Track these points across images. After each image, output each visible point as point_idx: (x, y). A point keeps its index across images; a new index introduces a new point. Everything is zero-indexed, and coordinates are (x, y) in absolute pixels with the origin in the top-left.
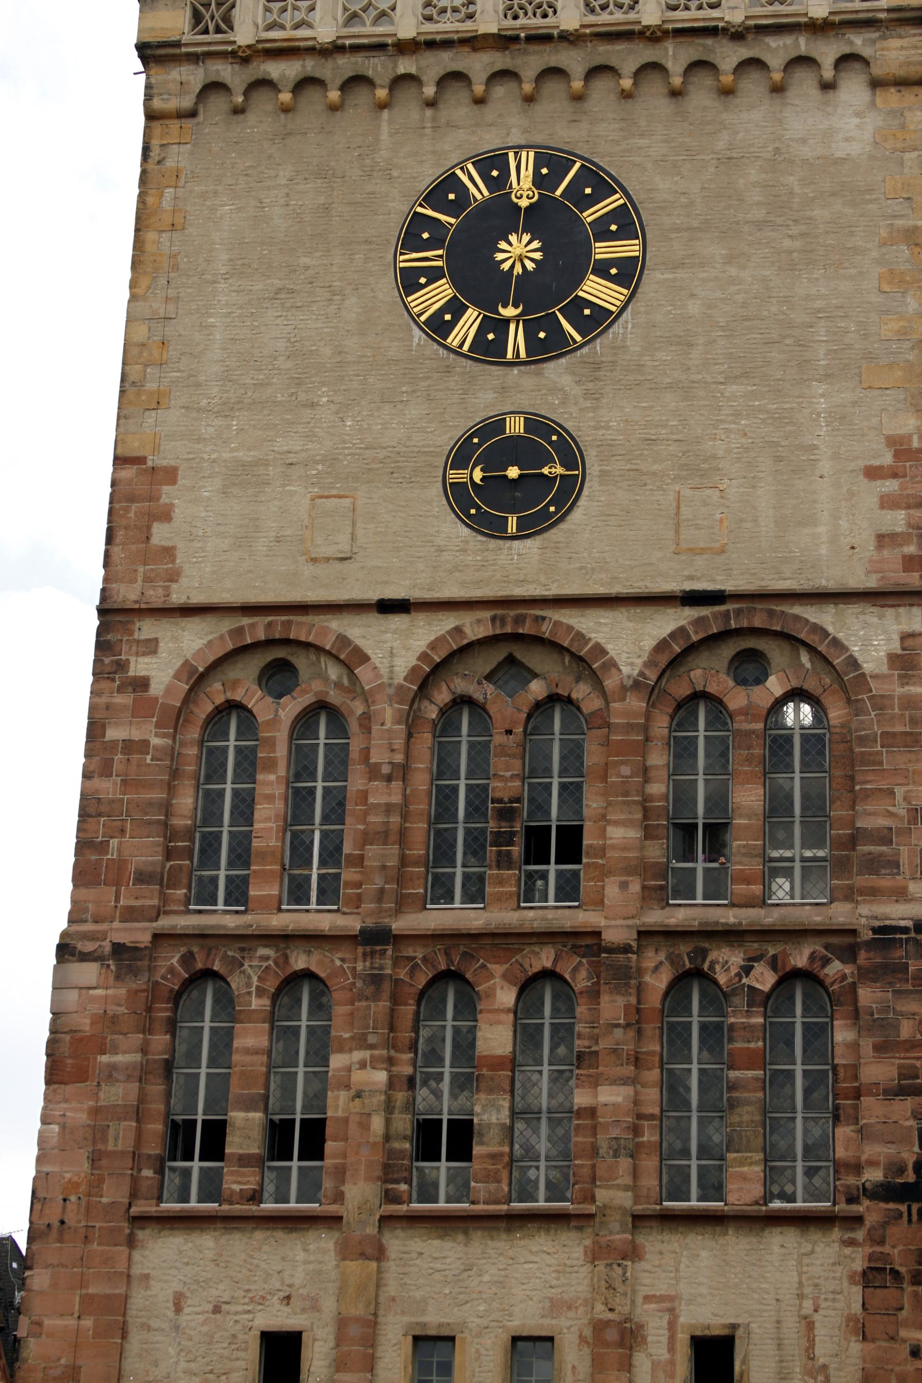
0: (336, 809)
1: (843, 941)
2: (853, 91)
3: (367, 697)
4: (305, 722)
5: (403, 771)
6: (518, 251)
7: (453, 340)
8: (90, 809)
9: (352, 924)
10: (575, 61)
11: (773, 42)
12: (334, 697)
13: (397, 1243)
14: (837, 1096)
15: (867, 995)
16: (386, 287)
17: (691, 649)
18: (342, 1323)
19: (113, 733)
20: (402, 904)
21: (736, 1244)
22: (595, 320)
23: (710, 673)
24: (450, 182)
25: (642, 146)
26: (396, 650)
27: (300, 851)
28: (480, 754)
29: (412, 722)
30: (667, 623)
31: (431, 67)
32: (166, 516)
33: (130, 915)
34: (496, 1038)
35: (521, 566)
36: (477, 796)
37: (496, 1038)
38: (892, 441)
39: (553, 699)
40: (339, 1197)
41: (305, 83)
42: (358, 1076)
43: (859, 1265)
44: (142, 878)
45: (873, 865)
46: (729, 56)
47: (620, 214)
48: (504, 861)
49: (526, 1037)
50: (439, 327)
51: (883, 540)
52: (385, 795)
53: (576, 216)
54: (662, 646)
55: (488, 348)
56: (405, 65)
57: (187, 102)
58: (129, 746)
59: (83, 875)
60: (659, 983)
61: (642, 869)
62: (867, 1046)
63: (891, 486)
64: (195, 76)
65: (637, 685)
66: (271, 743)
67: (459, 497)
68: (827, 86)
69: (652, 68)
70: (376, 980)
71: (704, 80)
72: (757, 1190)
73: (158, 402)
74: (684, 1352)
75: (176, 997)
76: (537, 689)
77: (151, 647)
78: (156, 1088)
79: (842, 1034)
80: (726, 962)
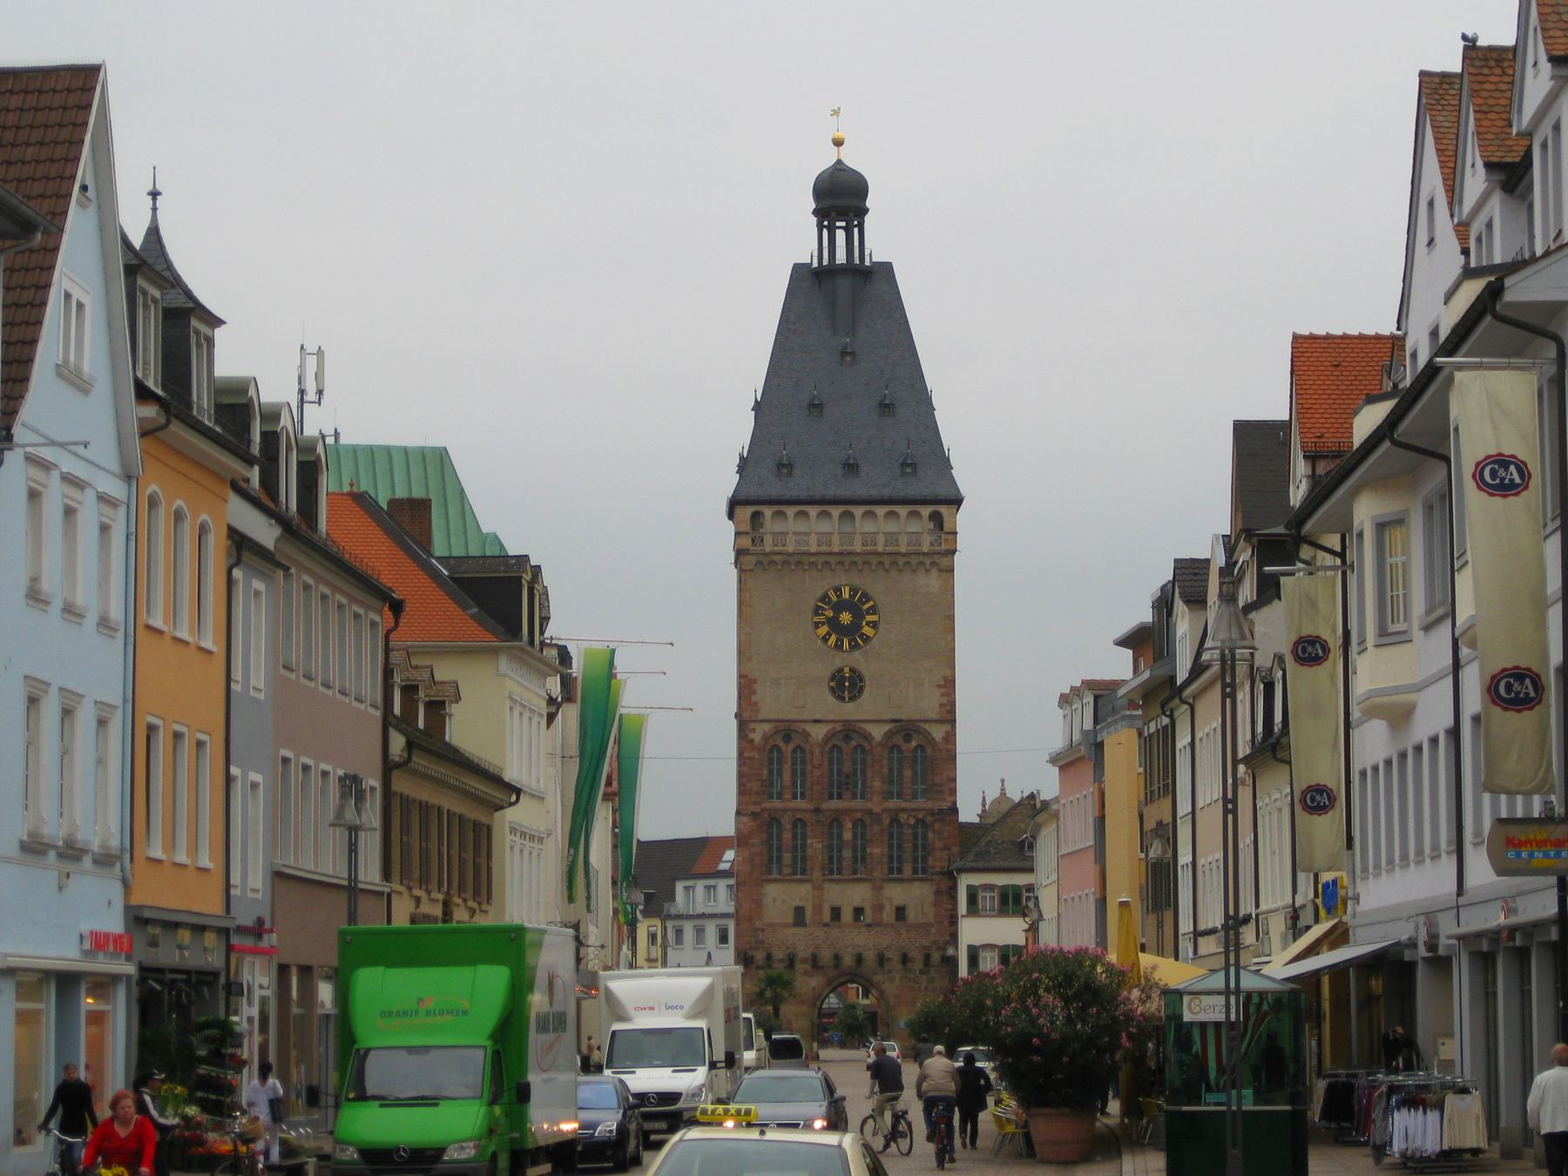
0: (803, 774)
1: (932, 813)
2: (934, 573)
4: (794, 751)
6: (846, 618)
8: (740, 775)
9: (810, 806)
10: (859, 559)
13: (826, 885)
15: (937, 826)
16: (810, 626)
21: (906, 886)
22: (867, 639)
23: (898, 740)
24: (826, 595)
26: (818, 732)
27: (794, 784)
28: (839, 760)
29: (822, 753)
33: (755, 803)
34: (848, 835)
35: (850, 711)
36: (839, 771)
37: (848, 835)
41: (785, 562)
43: (933, 889)
44: (757, 793)
46: (901, 561)
50: (825, 639)
51: (941, 705)
52: (817, 772)
53: (858, 605)
55: (839, 647)
56: (812, 559)
60: (887, 822)
64: (753, 559)
67: (832, 690)
68: (927, 571)
69: (881, 563)
73: (750, 659)
77: (754, 730)
79: (930, 835)
80: (903, 817)
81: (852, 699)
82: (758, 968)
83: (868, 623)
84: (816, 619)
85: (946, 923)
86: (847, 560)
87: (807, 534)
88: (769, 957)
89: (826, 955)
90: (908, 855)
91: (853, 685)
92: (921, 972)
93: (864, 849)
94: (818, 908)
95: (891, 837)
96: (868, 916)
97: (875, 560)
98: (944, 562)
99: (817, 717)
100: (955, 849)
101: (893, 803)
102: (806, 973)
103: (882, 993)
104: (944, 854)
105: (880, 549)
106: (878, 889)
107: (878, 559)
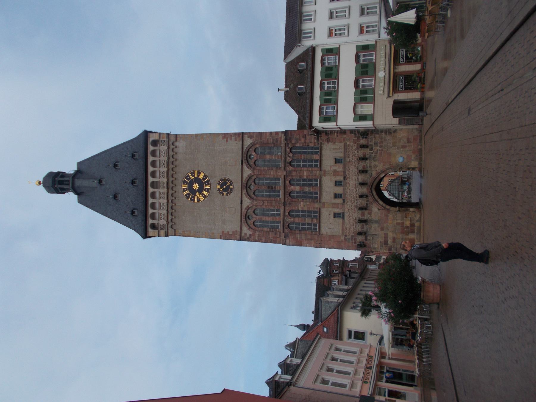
0: (268, 210)
1: (286, 145)
2: (177, 144)
3: (253, 206)
5: (263, 201)
6: (196, 186)
7: (207, 195)
9: (283, 207)
11: (170, 154)
12: (253, 210)
13: (323, 200)
14: (306, 146)
15: (293, 142)
17: (249, 164)
18: (333, 207)
19: (257, 239)
20: (280, 201)
21: (324, 158)
24: (186, 195)
25: (183, 170)
26: (247, 202)
29: (256, 200)
30: (245, 167)
31: (170, 198)
32: (228, 232)
33: (280, 236)
37: (297, 188)
38: (223, 139)
39: (254, 182)
40: (317, 208)
42: (302, 206)
44: (276, 234)
45: (277, 141)
46: (171, 159)
47: (191, 174)
48: (275, 188)
49: (298, 185)
50: (205, 197)
51: (236, 140)
52: (266, 204)
54: (248, 168)
55: (208, 190)
56: (170, 201)
57: (173, 230)
58: (258, 237)
59: (275, 242)
60: (291, 168)
61: (276, 170)
62: (300, 142)
63: (229, 139)
64: (170, 229)
65: (253, 171)
66: (259, 218)
68: (176, 147)
70: (290, 204)
71: (174, 163)
72: (317, 156)
74: (337, 165)
75: (291, 230)
76: (253, 184)
77: (246, 234)
78: (303, 232)
79: (298, 145)
80: (289, 159)
81: (231, 184)
82: (366, 239)
83: (194, 176)
84: (196, 201)
85: (345, 136)
86: (171, 185)
87: (160, 204)
88: (360, 234)
89: (361, 202)
90: (308, 157)
91: (225, 184)
92: (371, 149)
93: (304, 180)
94: (335, 205)
95: (299, 166)
96: (340, 178)
97: (171, 172)
98: (172, 139)
99: (240, 203)
100: (306, 132)
101: (282, 164)
102: (370, 213)
103: (383, 172)
104: (308, 137)
105: (166, 169)
106: (325, 173)
107: (171, 170)
